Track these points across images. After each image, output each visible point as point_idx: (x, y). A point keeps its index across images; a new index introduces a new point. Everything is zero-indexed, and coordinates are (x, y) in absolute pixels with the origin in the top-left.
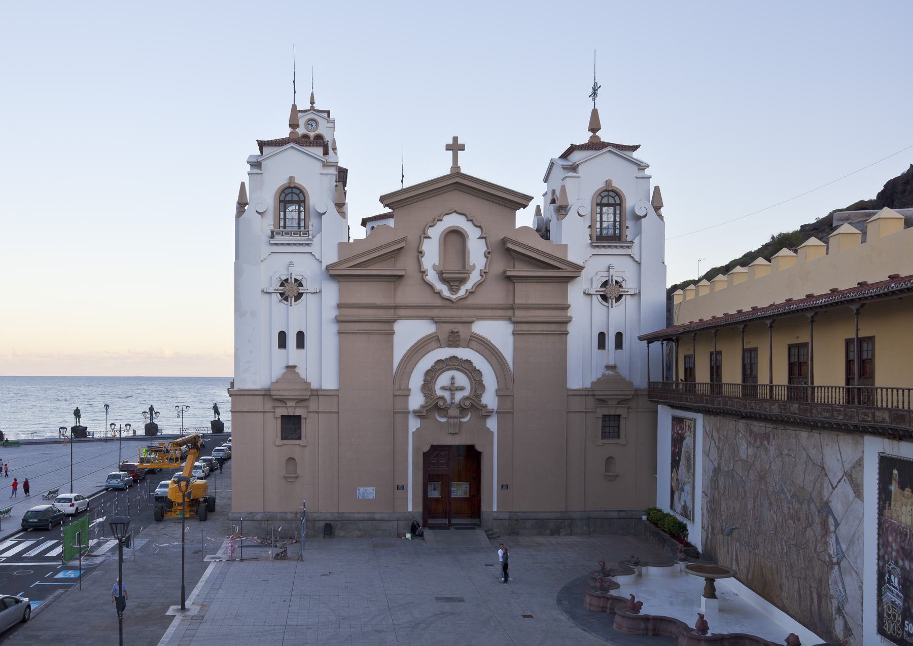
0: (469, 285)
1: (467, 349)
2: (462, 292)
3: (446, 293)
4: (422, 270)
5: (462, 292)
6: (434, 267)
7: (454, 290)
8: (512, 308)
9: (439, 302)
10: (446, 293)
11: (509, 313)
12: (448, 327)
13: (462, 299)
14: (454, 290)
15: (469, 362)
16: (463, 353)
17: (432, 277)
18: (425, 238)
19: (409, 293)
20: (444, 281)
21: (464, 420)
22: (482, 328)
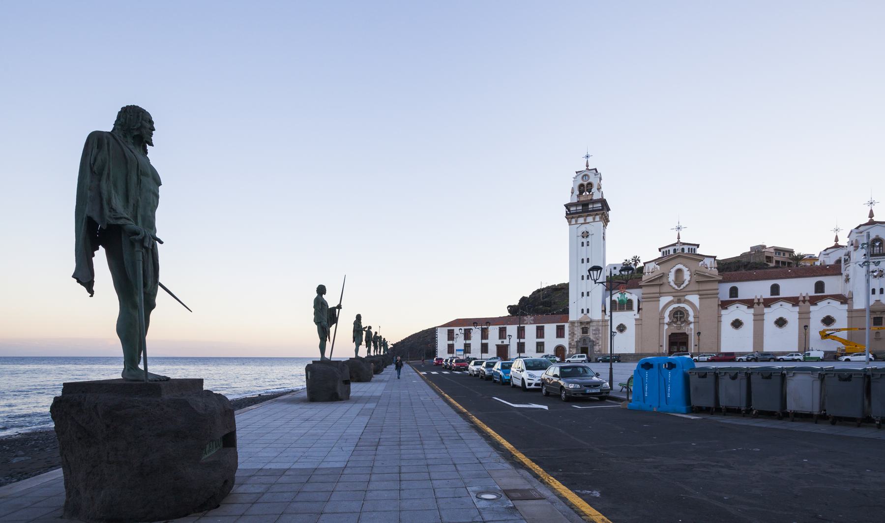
0: (684, 285)
2: (682, 287)
3: (677, 288)
5: (682, 287)
6: (673, 280)
7: (679, 287)
8: (698, 291)
9: (674, 291)
10: (677, 288)
12: (677, 298)
13: (681, 290)
15: (684, 308)
16: (682, 305)
17: (672, 284)
19: (665, 289)
20: (676, 284)
21: (682, 325)
22: (688, 298)
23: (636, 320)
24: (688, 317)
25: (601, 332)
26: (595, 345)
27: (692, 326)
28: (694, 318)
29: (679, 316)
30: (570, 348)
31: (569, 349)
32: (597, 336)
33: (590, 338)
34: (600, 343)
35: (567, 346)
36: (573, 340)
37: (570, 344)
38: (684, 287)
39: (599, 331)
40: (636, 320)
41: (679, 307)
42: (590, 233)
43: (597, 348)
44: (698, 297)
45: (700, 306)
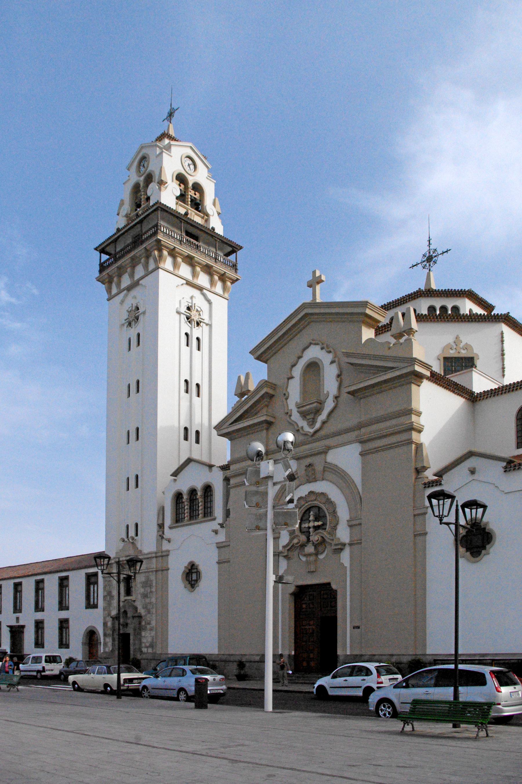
0: (323, 416)
1: (324, 482)
2: (318, 425)
4: (286, 411)
5: (318, 425)
7: (312, 423)
11: (353, 435)
13: (316, 432)
14: (312, 423)
16: (319, 487)
18: (289, 379)
22: (333, 457)
23: (220, 546)
24: (334, 528)
25: (154, 589)
26: (145, 629)
27: (345, 557)
28: (351, 526)
29: (311, 524)
30: (105, 635)
31: (104, 639)
32: (148, 600)
33: (136, 609)
34: (153, 623)
35: (100, 631)
36: (109, 614)
37: (105, 624)
38: (324, 423)
39: (151, 586)
40: (220, 546)
41: (311, 493)
42: (141, 310)
43: (147, 636)
44: (355, 449)
45: (363, 485)
